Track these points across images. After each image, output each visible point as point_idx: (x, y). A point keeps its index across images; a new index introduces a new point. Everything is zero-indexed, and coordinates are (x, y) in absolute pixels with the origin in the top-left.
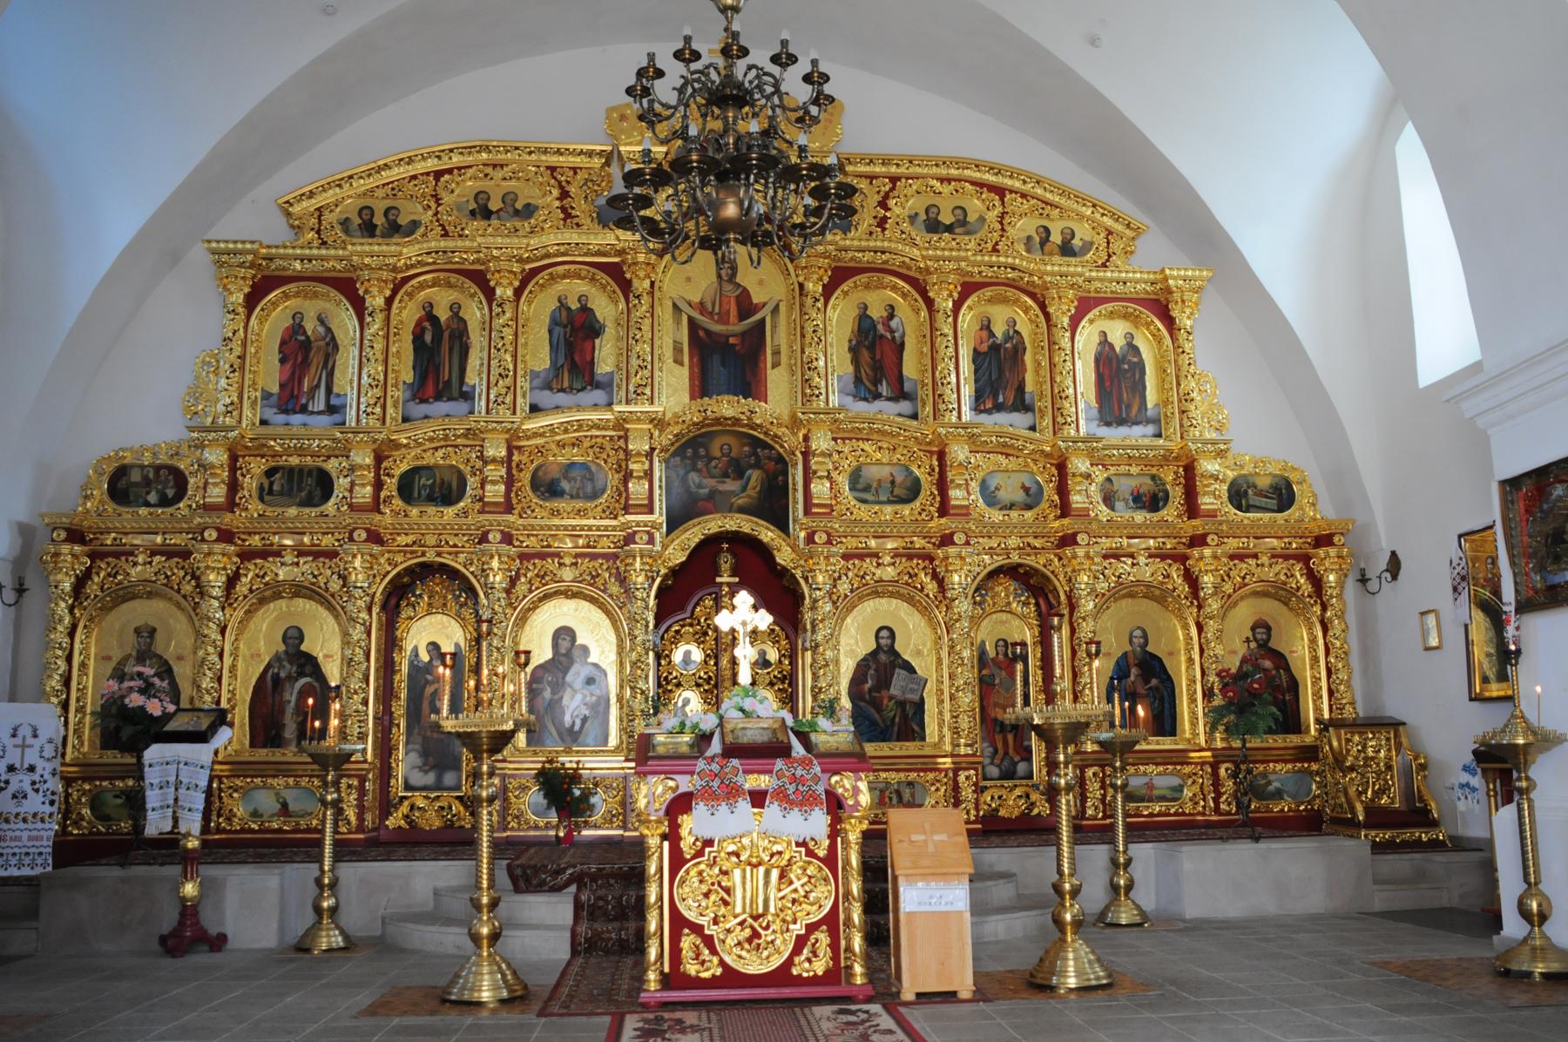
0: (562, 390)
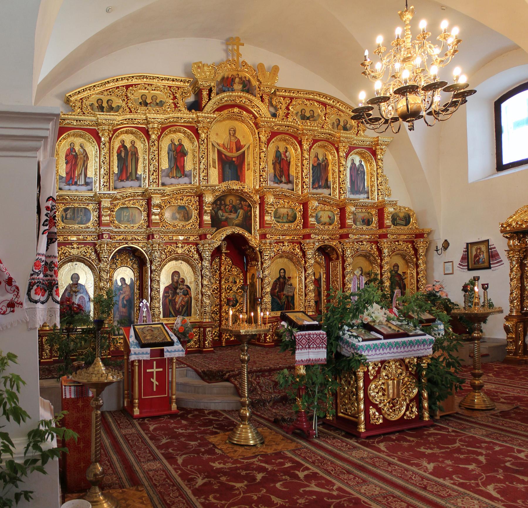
0: (173, 177)
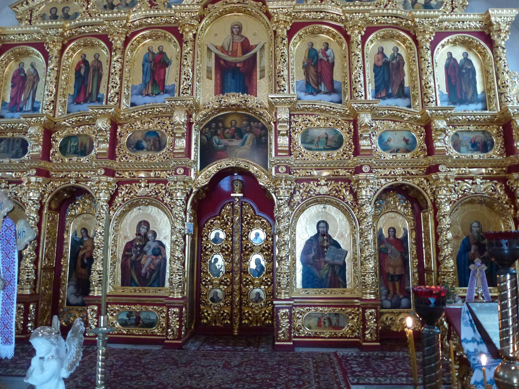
0: (148, 95)
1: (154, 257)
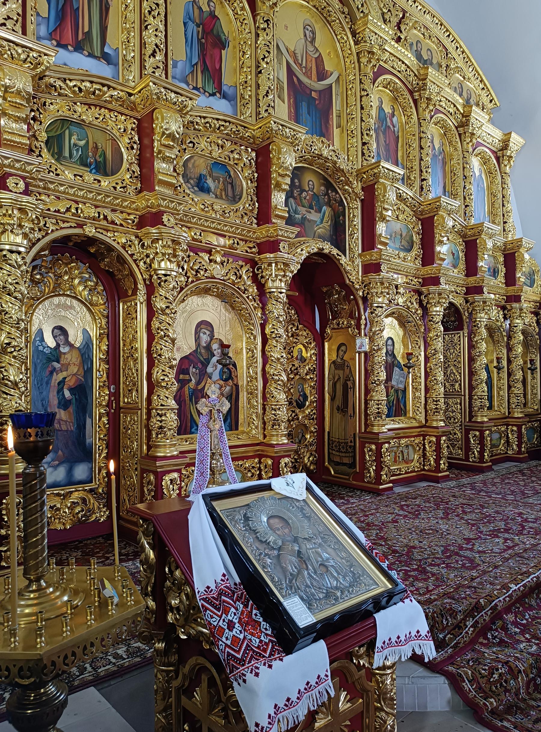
1: (222, 382)
